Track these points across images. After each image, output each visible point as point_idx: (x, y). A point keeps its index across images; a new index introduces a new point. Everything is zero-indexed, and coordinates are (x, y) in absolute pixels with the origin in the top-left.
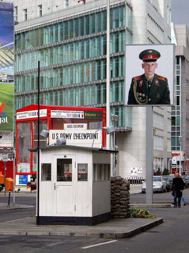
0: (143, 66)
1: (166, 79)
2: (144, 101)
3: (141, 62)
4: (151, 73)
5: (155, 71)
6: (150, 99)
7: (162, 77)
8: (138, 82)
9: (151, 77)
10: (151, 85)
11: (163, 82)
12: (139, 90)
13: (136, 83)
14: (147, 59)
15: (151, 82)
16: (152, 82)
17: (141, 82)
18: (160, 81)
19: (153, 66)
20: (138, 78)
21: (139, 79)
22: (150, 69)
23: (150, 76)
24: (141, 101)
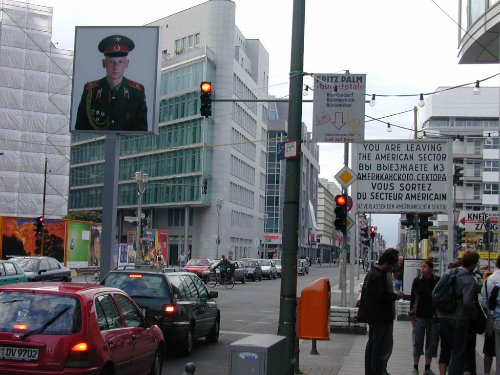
0: (105, 64)
1: (142, 87)
2: (103, 124)
3: (102, 56)
4: (117, 77)
5: (123, 72)
6: (113, 121)
7: (136, 83)
8: (95, 90)
9: (117, 82)
10: (117, 97)
11: (137, 94)
12: (96, 104)
13: (91, 93)
14: (112, 51)
15: (116, 91)
16: (118, 91)
17: (99, 92)
18: (132, 90)
19: (122, 65)
20: (95, 84)
21: (96, 85)
22: (115, 70)
23: (115, 81)
24: (98, 123)
